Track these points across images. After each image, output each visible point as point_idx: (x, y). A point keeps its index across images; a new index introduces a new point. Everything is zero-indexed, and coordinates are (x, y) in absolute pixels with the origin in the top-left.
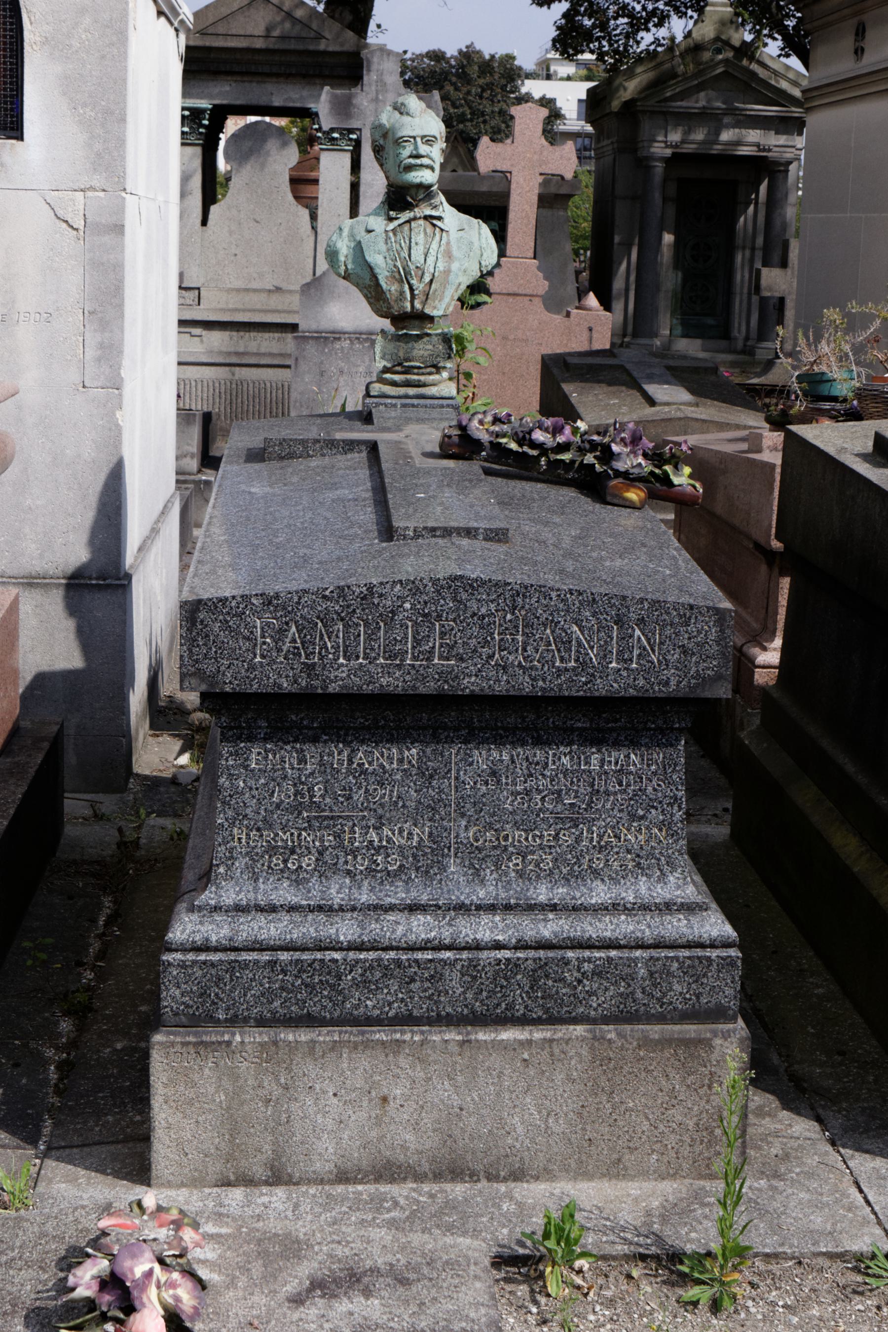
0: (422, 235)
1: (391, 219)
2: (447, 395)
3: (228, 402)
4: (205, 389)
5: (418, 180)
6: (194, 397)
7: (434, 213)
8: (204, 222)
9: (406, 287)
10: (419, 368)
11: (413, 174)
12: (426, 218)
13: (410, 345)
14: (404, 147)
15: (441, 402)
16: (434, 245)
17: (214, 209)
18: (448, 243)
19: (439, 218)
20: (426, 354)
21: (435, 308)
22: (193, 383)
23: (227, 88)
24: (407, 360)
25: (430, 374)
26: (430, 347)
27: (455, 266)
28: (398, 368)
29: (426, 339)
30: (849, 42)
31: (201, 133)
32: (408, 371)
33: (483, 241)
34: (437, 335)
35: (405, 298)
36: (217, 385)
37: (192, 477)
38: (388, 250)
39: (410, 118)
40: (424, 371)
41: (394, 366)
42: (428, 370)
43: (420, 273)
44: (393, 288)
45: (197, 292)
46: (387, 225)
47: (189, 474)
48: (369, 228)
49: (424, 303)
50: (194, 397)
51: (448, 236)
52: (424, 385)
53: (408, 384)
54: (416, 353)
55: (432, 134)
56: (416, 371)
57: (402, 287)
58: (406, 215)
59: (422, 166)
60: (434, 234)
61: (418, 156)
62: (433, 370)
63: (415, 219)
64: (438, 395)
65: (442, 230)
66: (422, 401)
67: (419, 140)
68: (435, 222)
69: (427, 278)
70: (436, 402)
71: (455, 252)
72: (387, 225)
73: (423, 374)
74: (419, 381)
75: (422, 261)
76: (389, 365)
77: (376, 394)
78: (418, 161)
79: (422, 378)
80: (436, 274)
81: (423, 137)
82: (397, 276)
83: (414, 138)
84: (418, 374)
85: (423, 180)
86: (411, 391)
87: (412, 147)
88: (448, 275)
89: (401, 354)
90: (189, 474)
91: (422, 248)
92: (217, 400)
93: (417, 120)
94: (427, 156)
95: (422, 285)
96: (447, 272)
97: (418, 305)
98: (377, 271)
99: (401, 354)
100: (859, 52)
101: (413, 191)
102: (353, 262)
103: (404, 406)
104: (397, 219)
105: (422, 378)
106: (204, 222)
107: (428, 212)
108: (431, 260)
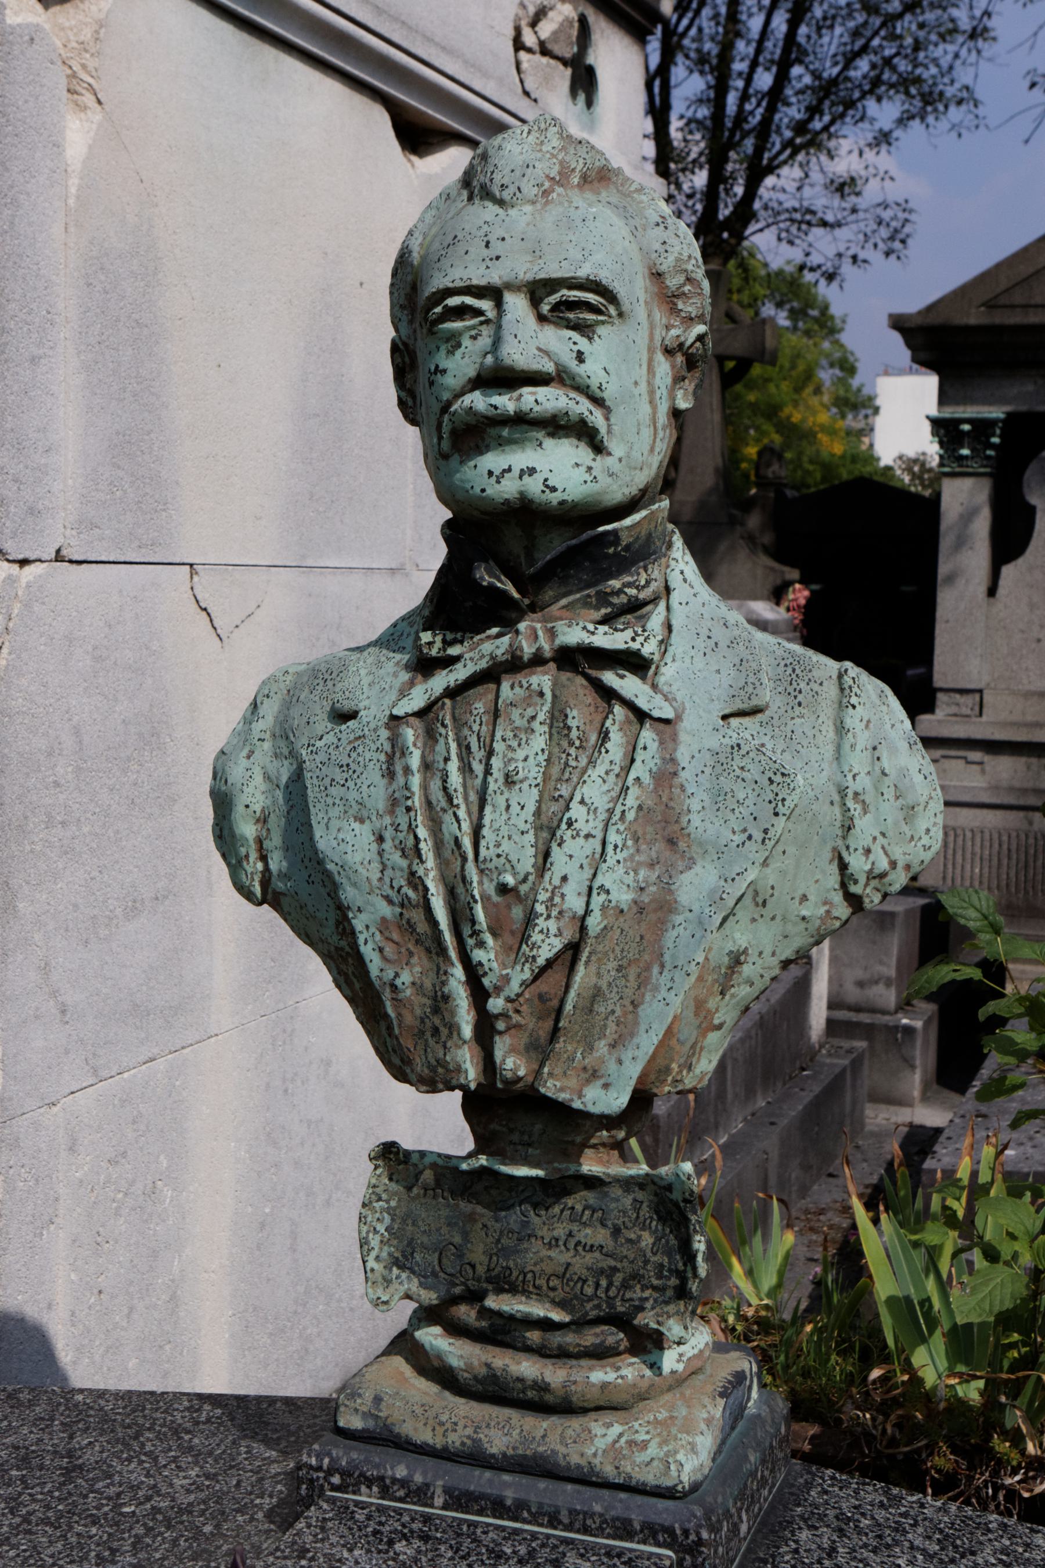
0: (539, 742)
1: (425, 666)
2: (650, 1477)
3: (1022, 864)
4: (988, 844)
5: (508, 489)
6: (968, 856)
8: (992, 592)
9: (458, 972)
10: (546, 1325)
11: (492, 460)
12: (572, 659)
13: (513, 1218)
14: (454, 341)
15: (620, 1504)
16: (596, 789)
17: (1008, 571)
18: (667, 775)
19: (635, 663)
20: (582, 1262)
21: (593, 1075)
22: (969, 835)
23: (1030, 388)
25: (600, 1354)
26: (600, 1236)
27: (695, 885)
28: (466, 1313)
29: (577, 1201)
31: (989, 457)
32: (501, 1332)
33: (858, 761)
34: (628, 1184)
35: (453, 1028)
36: (1005, 838)
37: (886, 1019)
38: (394, 803)
40: (569, 1339)
41: (455, 1300)
42: (590, 1338)
43: (517, 913)
44: (406, 977)
45: (977, 696)
47: (884, 1012)
48: (347, 706)
49: (542, 1050)
50: (968, 856)
52: (566, 1407)
53: (493, 1391)
54: (539, 1256)
55: (583, 272)
56: (534, 1336)
57: (442, 975)
58: (493, 645)
59: (522, 421)
60: (604, 736)
61: (502, 378)
62: (616, 1337)
63: (514, 665)
64: (609, 1471)
65: (641, 716)
66: (541, 1491)
69: (547, 943)
70: (599, 1503)
71: (701, 821)
72: (403, 693)
73: (562, 1354)
74: (542, 1387)
75: (527, 863)
78: (505, 402)
79: (556, 1375)
80: (595, 922)
81: (537, 290)
82: (422, 927)
83: (494, 293)
84: (542, 1352)
85: (533, 486)
86: (503, 1431)
87: (485, 341)
88: (661, 926)
89: (478, 1254)
90: (884, 1012)
92: (1005, 862)
93: (520, 216)
94: (561, 378)
95: (519, 976)
96: (655, 910)
97: (512, 1063)
98: (349, 894)
99: (478, 1254)
102: (287, 848)
103: (459, 1500)
104: (449, 662)
105: (556, 1375)
106: (992, 592)
107: (573, 635)
108: (570, 857)
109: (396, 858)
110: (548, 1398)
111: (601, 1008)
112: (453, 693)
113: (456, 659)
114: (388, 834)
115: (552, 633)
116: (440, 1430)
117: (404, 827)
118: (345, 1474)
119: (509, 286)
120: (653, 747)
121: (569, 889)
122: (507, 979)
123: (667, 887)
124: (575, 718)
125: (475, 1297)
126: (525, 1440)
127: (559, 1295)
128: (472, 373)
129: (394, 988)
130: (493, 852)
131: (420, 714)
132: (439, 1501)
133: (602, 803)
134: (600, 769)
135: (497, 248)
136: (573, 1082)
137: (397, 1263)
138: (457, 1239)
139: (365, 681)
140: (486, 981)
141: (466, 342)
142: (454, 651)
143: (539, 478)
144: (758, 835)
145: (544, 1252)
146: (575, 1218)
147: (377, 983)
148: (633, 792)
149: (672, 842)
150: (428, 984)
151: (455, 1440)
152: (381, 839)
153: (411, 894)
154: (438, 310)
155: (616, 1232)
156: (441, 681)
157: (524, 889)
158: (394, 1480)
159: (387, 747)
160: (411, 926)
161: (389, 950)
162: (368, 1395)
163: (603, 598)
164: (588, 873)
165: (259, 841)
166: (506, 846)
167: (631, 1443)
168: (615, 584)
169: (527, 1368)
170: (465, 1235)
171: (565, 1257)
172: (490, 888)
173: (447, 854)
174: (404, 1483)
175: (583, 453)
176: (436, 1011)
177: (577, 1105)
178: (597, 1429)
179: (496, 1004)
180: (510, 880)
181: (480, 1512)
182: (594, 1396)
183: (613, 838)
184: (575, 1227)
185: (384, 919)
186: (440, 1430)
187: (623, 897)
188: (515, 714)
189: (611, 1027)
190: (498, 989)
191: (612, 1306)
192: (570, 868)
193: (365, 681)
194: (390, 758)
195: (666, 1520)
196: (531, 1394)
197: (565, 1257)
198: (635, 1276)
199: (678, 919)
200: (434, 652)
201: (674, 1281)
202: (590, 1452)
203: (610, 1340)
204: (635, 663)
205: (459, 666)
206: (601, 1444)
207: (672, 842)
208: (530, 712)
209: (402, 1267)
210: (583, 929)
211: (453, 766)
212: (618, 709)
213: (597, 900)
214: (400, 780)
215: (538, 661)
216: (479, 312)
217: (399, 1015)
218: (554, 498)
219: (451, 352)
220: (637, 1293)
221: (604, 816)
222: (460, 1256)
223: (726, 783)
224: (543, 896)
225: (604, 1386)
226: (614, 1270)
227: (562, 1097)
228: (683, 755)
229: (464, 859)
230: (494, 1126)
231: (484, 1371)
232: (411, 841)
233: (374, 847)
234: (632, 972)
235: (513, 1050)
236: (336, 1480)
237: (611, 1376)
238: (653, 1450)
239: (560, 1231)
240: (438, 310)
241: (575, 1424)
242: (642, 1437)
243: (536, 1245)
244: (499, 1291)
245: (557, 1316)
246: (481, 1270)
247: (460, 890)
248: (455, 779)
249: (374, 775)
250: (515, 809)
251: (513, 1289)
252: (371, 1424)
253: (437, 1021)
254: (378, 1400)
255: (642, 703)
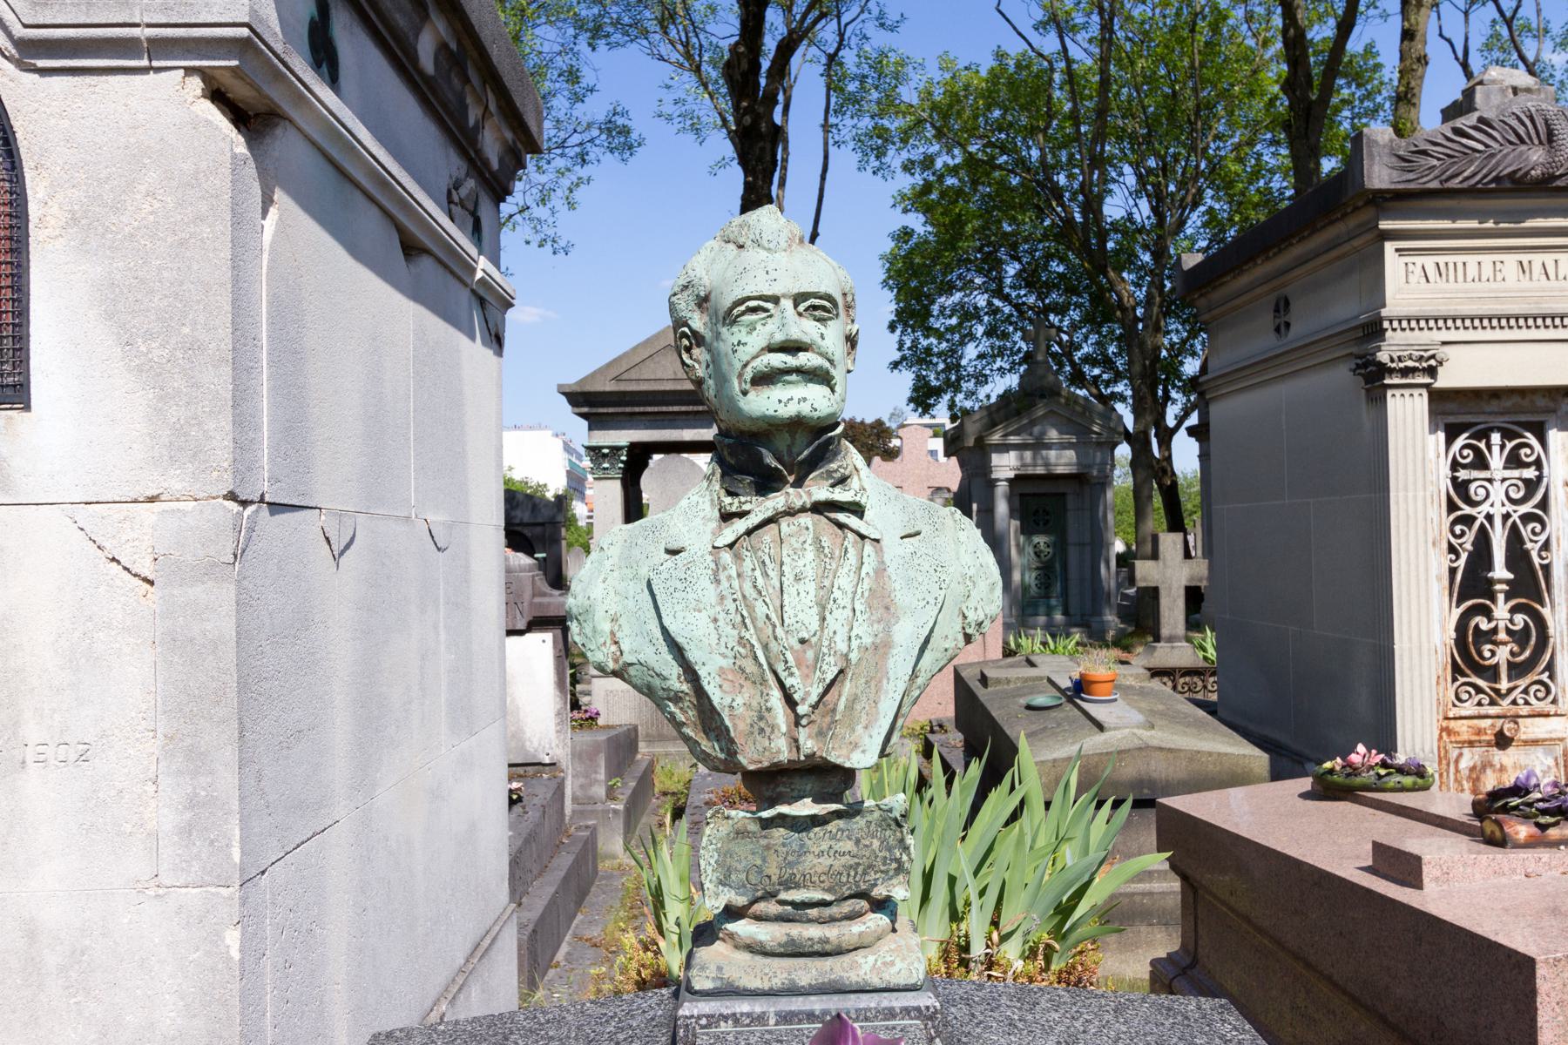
0: (810, 554)
2: (902, 981)
7: (840, 495)
9: (776, 696)
12: (819, 508)
15: (888, 1001)
16: (845, 580)
18: (881, 571)
19: (857, 509)
20: (839, 863)
24: (789, 884)
25: (852, 916)
26: (849, 846)
30: (1267, 320)
35: (773, 727)
39: (763, 254)
40: (834, 910)
42: (846, 907)
43: (810, 654)
44: (739, 700)
46: (717, 533)
48: (674, 546)
51: (879, 552)
52: (839, 952)
53: (794, 951)
54: (814, 863)
55: (823, 289)
57: (765, 696)
63: (791, 512)
65: (863, 537)
67: (787, 304)
68: (842, 517)
71: (902, 596)
72: (717, 533)
73: (833, 920)
75: (815, 625)
76: (741, 901)
77: (708, 985)
79: (832, 933)
80: (854, 656)
81: (798, 299)
83: (775, 300)
85: (805, 409)
86: (807, 972)
88: (885, 656)
89: (773, 870)
91: (811, 587)
96: (881, 648)
99: (773, 870)
100: (1281, 328)
101: (782, 442)
103: (785, 1018)
104: (742, 514)
105: (832, 933)
108: (837, 620)
109: (729, 629)
110: (828, 948)
111: (858, 707)
112: (749, 533)
113: (747, 513)
114: (721, 616)
115: (809, 494)
116: (766, 979)
117: (733, 610)
118: (708, 1016)
119: (784, 296)
120: (873, 555)
121: (838, 638)
122: (808, 693)
123: (888, 631)
124: (826, 542)
125: (770, 895)
126: (821, 974)
127: (826, 885)
128: (764, 344)
129: (731, 707)
130: (793, 620)
131: (731, 546)
132: (772, 1022)
133: (849, 589)
134: (846, 569)
135: (773, 275)
136: (844, 752)
137: (721, 883)
138: (759, 862)
139: (684, 530)
140: (796, 697)
141: (759, 326)
142: (746, 507)
143: (808, 403)
144: (932, 601)
145: (816, 861)
146: (833, 837)
147: (718, 708)
148: (866, 581)
149: (887, 608)
150: (754, 704)
151: (777, 983)
152: (715, 620)
153: (742, 650)
154: (742, 308)
155: (858, 842)
156: (741, 526)
157: (814, 640)
158: (742, 1014)
159: (713, 566)
160: (742, 670)
161: (726, 686)
162: (713, 967)
163: (829, 474)
164: (846, 629)
165: (613, 633)
166: (801, 616)
167: (884, 964)
168: (834, 466)
169: (814, 932)
170: (764, 860)
171: (830, 861)
172: (794, 642)
173: (760, 624)
174: (748, 1015)
175: (826, 390)
176: (761, 718)
177: (847, 765)
178: (861, 960)
179: (802, 709)
180: (806, 636)
181: (800, 1022)
182: (854, 941)
183: (858, 607)
184: (833, 843)
185: (721, 668)
186: (766, 979)
187: (867, 640)
188: (793, 540)
189: (864, 716)
190: (803, 699)
191: (858, 886)
192: (837, 627)
193: (684, 530)
194: (716, 573)
195: (915, 1003)
196: (817, 947)
197: (830, 861)
198: (871, 866)
199: (894, 651)
200: (734, 509)
201: (894, 865)
202: (862, 973)
203: (857, 908)
204: (857, 509)
205: (752, 516)
206: (866, 968)
207: (887, 608)
208: (802, 539)
209: (724, 885)
210: (848, 660)
211: (758, 573)
212: (850, 535)
213: (855, 643)
214: (724, 584)
215: (803, 510)
216: (766, 310)
217: (735, 725)
218: (816, 415)
219: (749, 333)
220: (872, 876)
221: (850, 595)
222: (760, 872)
223: (912, 573)
224: (826, 643)
225: (860, 934)
226: (858, 864)
227: (839, 761)
228: (887, 558)
229: (774, 626)
230: (781, 789)
231: (785, 939)
232: (739, 618)
233: (712, 625)
234: (873, 684)
235: (810, 737)
236: (704, 1022)
237: (863, 928)
238: (899, 965)
239: (824, 847)
240: (742, 308)
241: (846, 959)
242: (888, 959)
243: (810, 857)
244: (788, 889)
245: (829, 897)
246: (774, 878)
247: (773, 645)
248: (760, 582)
249: (705, 582)
250: (803, 594)
251: (797, 886)
252: (718, 984)
253: (762, 724)
254: (720, 969)
255: (863, 531)
